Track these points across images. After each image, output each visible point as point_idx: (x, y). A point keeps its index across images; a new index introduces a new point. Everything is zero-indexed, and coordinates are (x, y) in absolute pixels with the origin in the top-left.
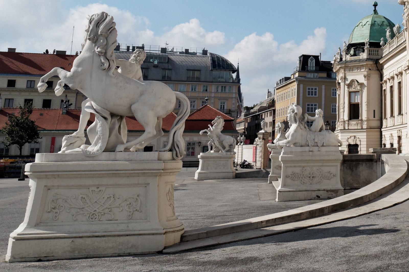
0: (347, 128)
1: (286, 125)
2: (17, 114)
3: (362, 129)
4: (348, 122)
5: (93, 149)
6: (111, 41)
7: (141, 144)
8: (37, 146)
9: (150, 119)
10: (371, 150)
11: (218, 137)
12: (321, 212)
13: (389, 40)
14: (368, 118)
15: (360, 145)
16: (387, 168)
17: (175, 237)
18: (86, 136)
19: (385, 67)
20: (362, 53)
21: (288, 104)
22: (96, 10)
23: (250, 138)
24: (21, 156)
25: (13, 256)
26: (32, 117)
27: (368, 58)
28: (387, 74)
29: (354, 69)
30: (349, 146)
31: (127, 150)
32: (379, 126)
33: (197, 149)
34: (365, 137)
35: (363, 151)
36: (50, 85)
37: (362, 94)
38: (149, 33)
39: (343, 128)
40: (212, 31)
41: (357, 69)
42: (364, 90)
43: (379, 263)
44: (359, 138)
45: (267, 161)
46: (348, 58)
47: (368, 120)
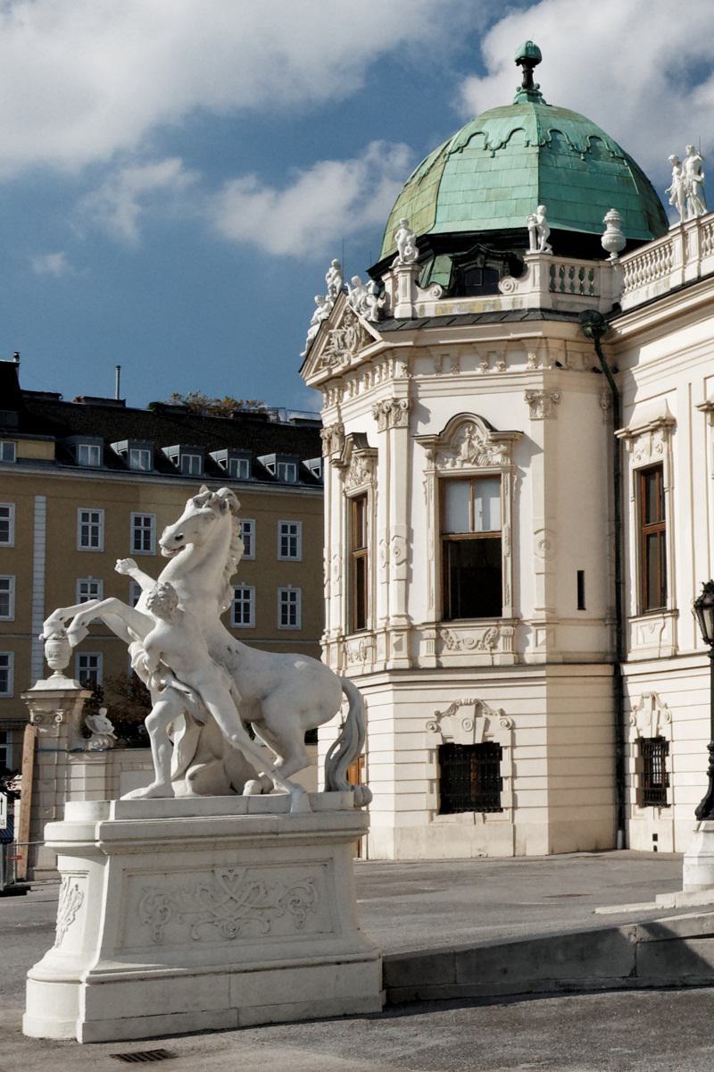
0: (427, 660)
3: (520, 664)
4: (438, 629)
14: (550, 610)
15: (513, 746)
19: (647, 353)
20: (511, 281)
27: (549, 306)
29: (465, 360)
32: (606, 653)
34: (542, 706)
37: (518, 492)
39: (405, 664)
41: (483, 359)
42: (524, 469)
44: (502, 713)
47: (552, 622)
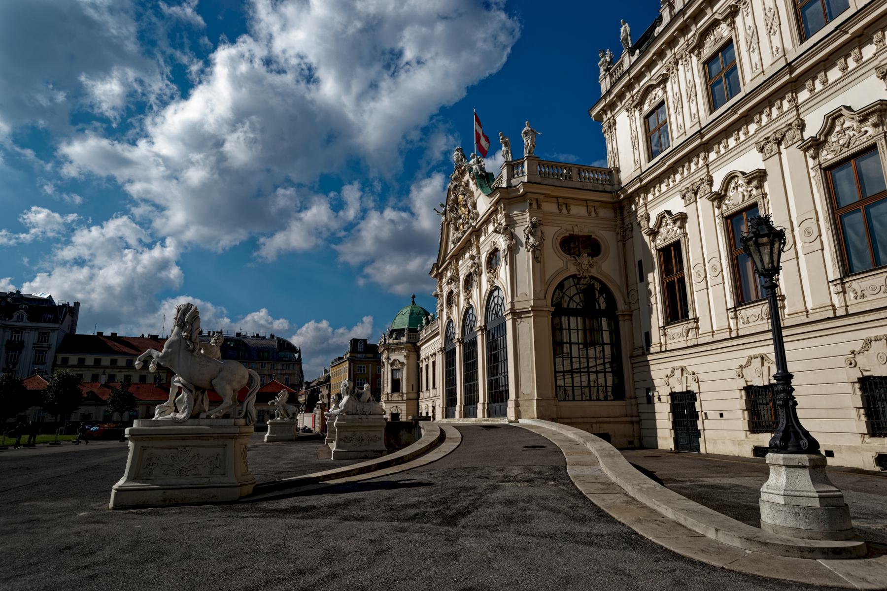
1: (340, 397)
2: (119, 387)
5: (181, 416)
6: (195, 327)
7: (220, 413)
8: (135, 413)
9: (228, 393)
10: (410, 418)
11: (284, 406)
12: (368, 469)
13: (425, 326)
16: (423, 433)
17: (249, 489)
18: (175, 405)
21: (341, 379)
22: (183, 301)
23: (309, 409)
24: (122, 422)
25: (115, 504)
26: (130, 390)
28: (423, 355)
30: (392, 414)
31: (208, 417)
33: (266, 416)
35: (403, 418)
36: (146, 363)
38: (227, 320)
40: (278, 319)
43: (417, 511)
45: (324, 427)
46: (391, 341)
47: (407, 393)
